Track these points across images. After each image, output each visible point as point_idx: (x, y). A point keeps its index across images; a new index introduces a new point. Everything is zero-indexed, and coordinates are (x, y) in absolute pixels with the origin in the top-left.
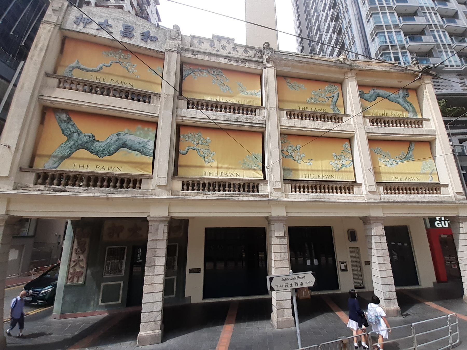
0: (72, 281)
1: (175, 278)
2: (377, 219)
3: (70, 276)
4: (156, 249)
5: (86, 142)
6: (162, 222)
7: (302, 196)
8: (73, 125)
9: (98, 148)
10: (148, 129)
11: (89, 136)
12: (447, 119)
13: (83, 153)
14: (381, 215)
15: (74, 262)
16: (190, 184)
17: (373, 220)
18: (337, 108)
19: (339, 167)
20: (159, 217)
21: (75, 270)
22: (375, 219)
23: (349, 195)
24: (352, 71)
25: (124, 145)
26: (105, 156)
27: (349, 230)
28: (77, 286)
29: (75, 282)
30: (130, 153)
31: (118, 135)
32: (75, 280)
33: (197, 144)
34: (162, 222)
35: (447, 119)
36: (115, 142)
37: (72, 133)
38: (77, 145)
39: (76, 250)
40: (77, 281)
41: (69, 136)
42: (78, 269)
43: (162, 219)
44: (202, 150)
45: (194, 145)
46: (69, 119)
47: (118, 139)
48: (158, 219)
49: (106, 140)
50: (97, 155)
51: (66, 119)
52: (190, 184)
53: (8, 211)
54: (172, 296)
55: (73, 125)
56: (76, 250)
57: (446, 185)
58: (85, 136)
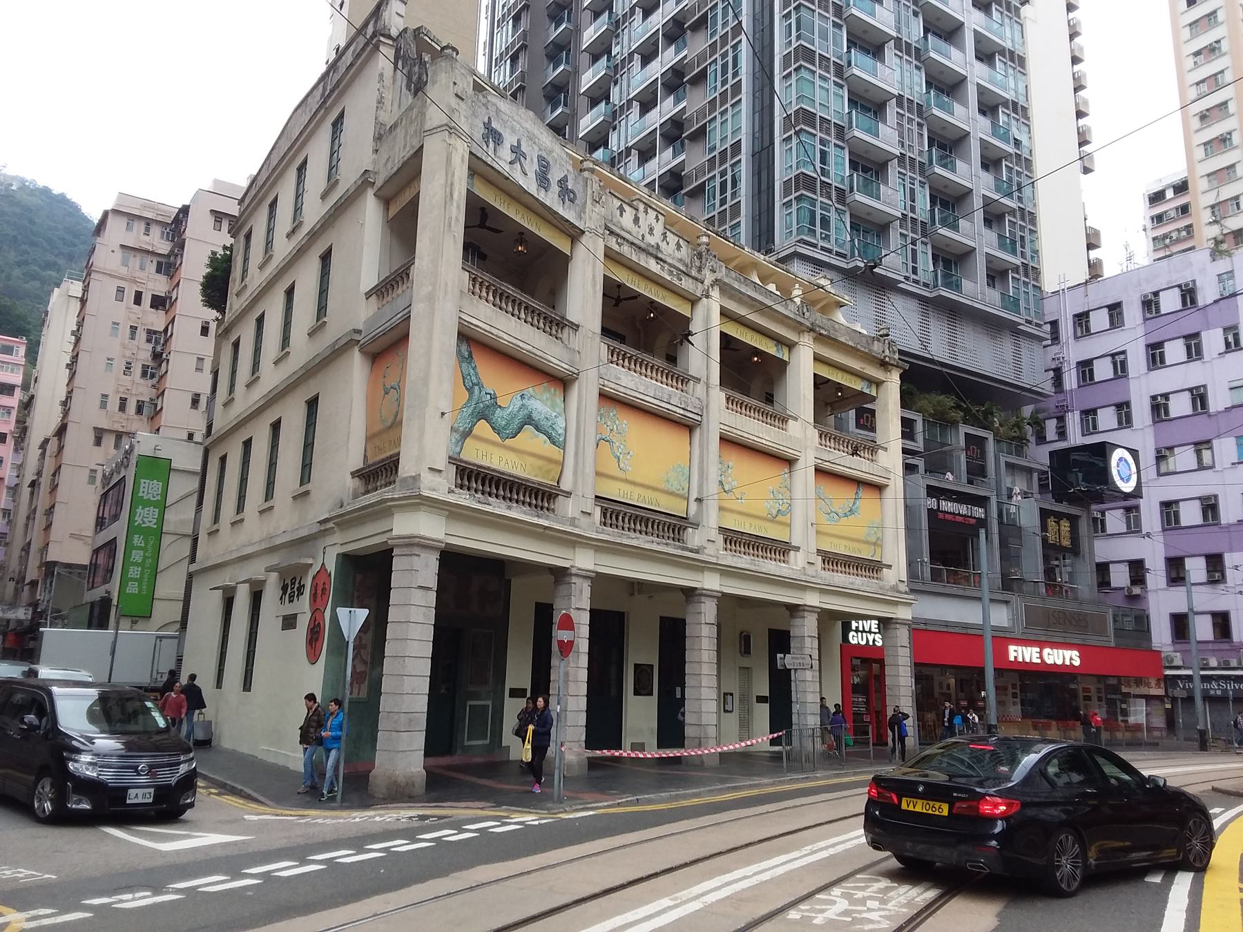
1: (489, 703)
5: (488, 406)
7: (735, 559)
8: (474, 368)
9: (499, 420)
10: (555, 391)
11: (490, 394)
13: (483, 428)
17: (807, 611)
19: (774, 512)
23: (783, 565)
24: (811, 333)
25: (529, 420)
26: (507, 438)
27: (742, 633)
30: (537, 436)
31: (522, 396)
33: (611, 430)
36: (519, 411)
37: (474, 384)
38: (477, 410)
40: (359, 694)
41: (470, 390)
44: (617, 444)
45: (606, 434)
46: (470, 356)
47: (522, 405)
49: (509, 406)
50: (499, 434)
51: (466, 354)
54: (480, 742)
55: (474, 368)
57: (889, 567)
58: (486, 393)
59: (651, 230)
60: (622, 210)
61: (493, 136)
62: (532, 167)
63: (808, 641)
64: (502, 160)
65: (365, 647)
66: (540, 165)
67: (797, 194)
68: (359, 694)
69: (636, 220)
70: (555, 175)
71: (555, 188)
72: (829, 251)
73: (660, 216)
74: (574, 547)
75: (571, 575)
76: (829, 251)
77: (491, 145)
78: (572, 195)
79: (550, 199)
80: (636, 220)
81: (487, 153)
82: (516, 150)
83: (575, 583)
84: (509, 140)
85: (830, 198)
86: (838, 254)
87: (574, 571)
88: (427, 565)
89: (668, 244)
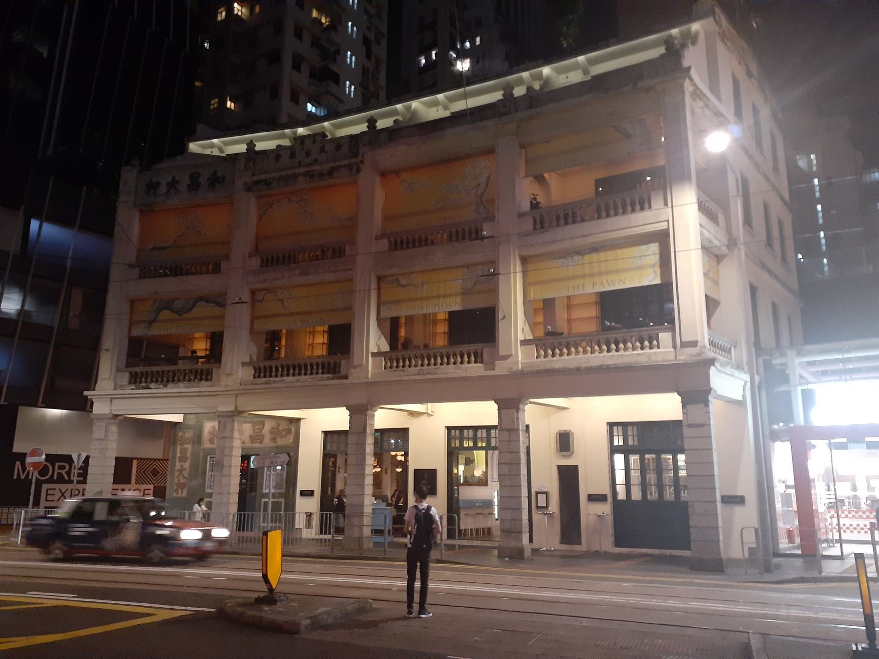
0: (177, 494)
3: (175, 487)
15: (178, 471)
18: (484, 207)
21: (179, 480)
28: (182, 499)
29: (180, 495)
32: (180, 491)
39: (179, 457)
40: (182, 494)
42: (182, 481)
43: (229, 414)
53: (111, 410)
65: (185, 469)
68: (182, 494)
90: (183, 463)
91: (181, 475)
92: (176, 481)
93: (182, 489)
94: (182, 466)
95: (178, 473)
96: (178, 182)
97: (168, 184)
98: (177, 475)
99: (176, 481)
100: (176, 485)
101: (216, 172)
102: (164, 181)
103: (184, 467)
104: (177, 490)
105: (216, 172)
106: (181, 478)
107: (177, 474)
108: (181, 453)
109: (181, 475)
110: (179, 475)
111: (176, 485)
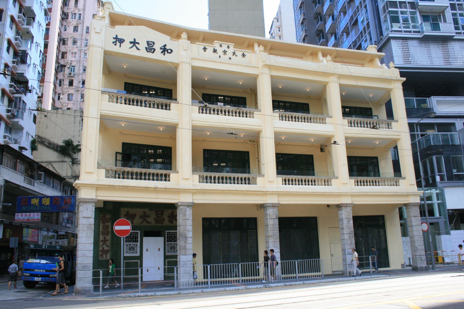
0: (102, 257)
2: (346, 205)
3: (100, 253)
4: (186, 225)
6: (188, 206)
12: (415, 121)
14: (350, 202)
15: (102, 241)
16: (217, 178)
17: (343, 206)
20: (187, 203)
21: (103, 248)
22: (345, 205)
29: (104, 258)
32: (104, 256)
34: (188, 206)
35: (415, 121)
40: (106, 258)
42: (106, 248)
48: (186, 204)
52: (217, 178)
56: (102, 232)
59: (225, 52)
60: (205, 49)
61: (119, 41)
62: (143, 45)
63: (345, 222)
64: (125, 49)
65: (108, 240)
66: (148, 44)
67: (388, 10)
69: (215, 51)
70: (157, 47)
71: (158, 51)
72: (410, 32)
73: (230, 46)
74: (180, 194)
75: (179, 206)
76: (410, 32)
77: (118, 44)
78: (169, 51)
79: (158, 55)
80: (215, 51)
81: (116, 49)
82: (134, 43)
83: (182, 209)
84: (128, 39)
85: (406, 8)
86: (414, 32)
87: (179, 204)
88: (87, 209)
89: (237, 56)
90: (105, 236)
91: (105, 244)
92: (101, 249)
93: (106, 254)
94: (105, 238)
95: (102, 243)
96: (138, 43)
97: (131, 43)
98: (101, 245)
99: (101, 249)
100: (101, 251)
101: (165, 45)
102: (128, 39)
103: (106, 239)
104: (102, 255)
105: (165, 45)
106: (105, 246)
107: (101, 243)
108: (103, 229)
109: (105, 244)
110: (103, 245)
111: (101, 251)
